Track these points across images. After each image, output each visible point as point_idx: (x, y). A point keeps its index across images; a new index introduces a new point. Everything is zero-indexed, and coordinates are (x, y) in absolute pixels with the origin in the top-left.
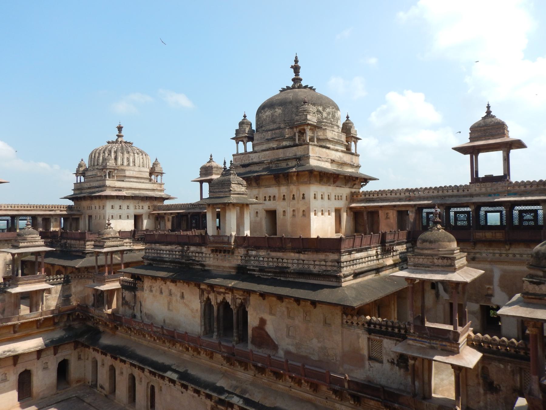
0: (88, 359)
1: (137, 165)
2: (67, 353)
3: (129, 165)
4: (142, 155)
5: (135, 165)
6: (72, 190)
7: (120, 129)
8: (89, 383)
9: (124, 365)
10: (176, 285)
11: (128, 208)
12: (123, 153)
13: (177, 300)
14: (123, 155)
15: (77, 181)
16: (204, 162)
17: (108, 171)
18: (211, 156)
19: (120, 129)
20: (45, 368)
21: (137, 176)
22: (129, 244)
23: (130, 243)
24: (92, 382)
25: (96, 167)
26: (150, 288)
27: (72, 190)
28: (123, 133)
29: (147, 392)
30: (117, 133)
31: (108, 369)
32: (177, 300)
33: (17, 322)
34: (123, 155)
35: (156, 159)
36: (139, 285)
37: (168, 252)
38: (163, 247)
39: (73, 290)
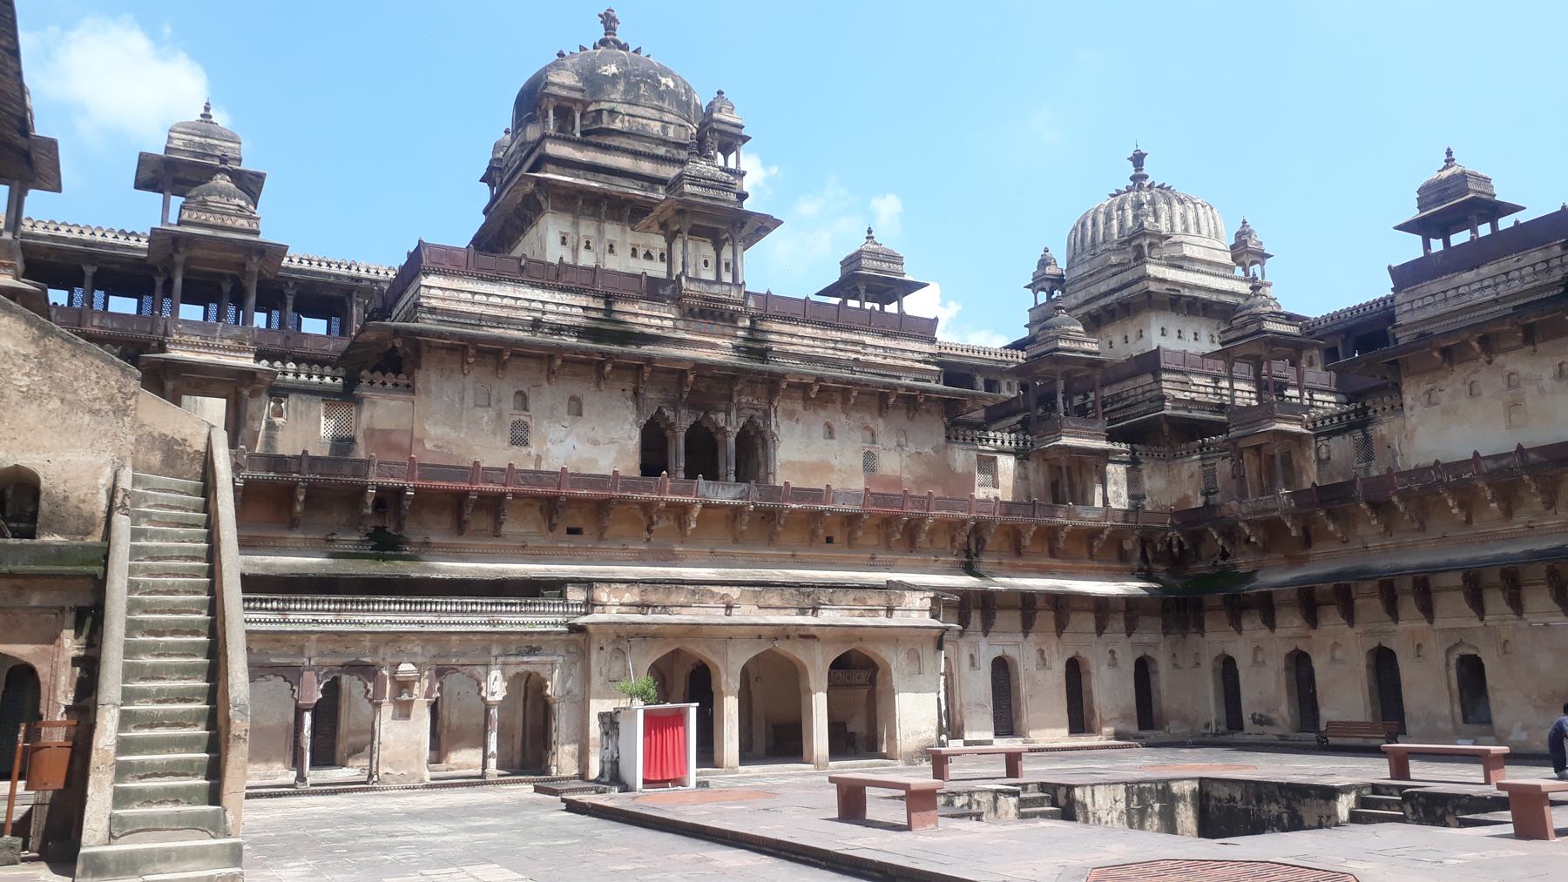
0: (1198, 664)
1: (1205, 232)
2: (1150, 638)
3: (1186, 230)
4: (1212, 209)
5: (1199, 232)
6: (1026, 326)
7: (1138, 159)
8: (1207, 726)
9: (1350, 632)
10: (1535, 351)
11: (1196, 339)
12: (1169, 204)
13: (1541, 391)
14: (1170, 208)
15: (1036, 302)
16: (1432, 171)
17: (1148, 242)
18: (1449, 153)
19: (1138, 159)
20: (1113, 663)
21: (1209, 258)
22: (1247, 395)
23: (1250, 392)
24: (1218, 723)
25: (1103, 248)
26: (1427, 396)
27: (1026, 326)
28: (1146, 169)
29: (1448, 677)
30: (1132, 171)
31: (1282, 666)
32: (1541, 391)
33: (1065, 521)
34: (1170, 208)
35: (1244, 222)
36: (1379, 409)
37: (1491, 282)
38: (1468, 276)
39: (1147, 484)
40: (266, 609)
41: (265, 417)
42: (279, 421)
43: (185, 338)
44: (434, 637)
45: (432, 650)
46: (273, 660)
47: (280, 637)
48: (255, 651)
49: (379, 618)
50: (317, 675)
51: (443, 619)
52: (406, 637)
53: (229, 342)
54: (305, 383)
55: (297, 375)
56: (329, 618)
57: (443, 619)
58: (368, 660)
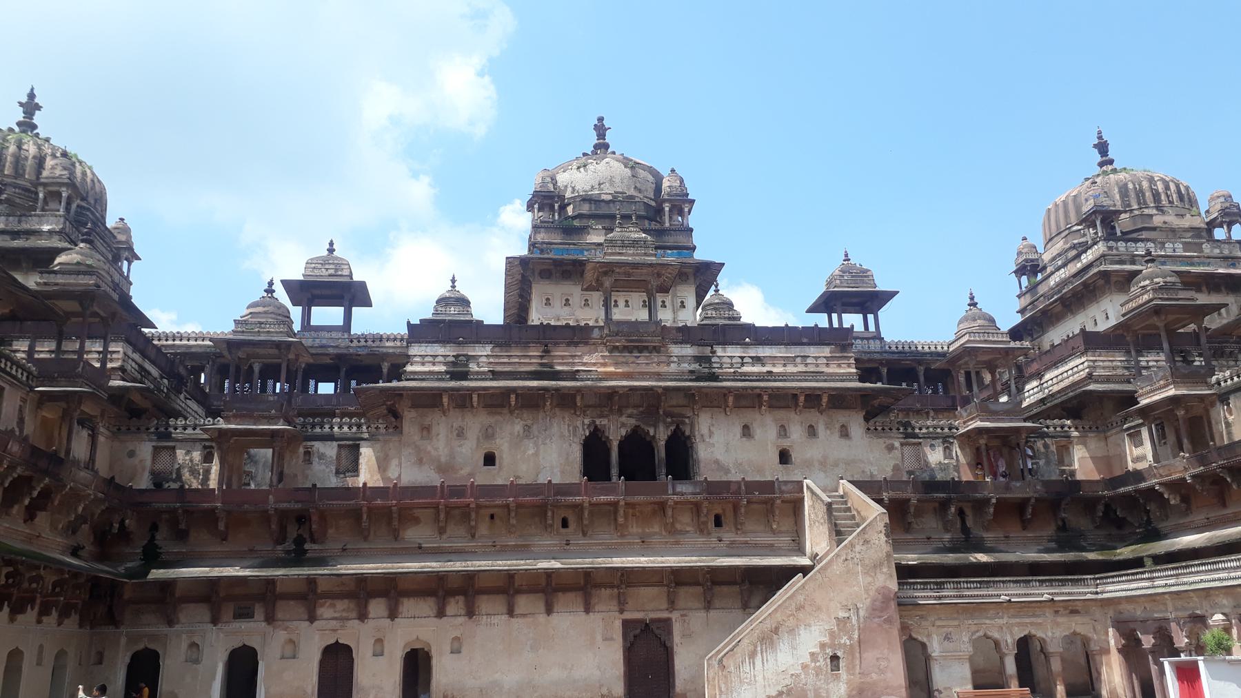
40: (1144, 579)
41: (1223, 419)
42: (1230, 418)
43: (1144, 390)
44: (1027, 605)
45: (1111, 613)
46: (1156, 615)
47: (1154, 598)
48: (1148, 609)
49: (1197, 578)
50: (1178, 624)
51: (1233, 575)
52: (1212, 592)
53: (1162, 382)
54: (1232, 385)
55: (1232, 379)
56: (1172, 581)
57: (1233, 575)
58: (1198, 612)
